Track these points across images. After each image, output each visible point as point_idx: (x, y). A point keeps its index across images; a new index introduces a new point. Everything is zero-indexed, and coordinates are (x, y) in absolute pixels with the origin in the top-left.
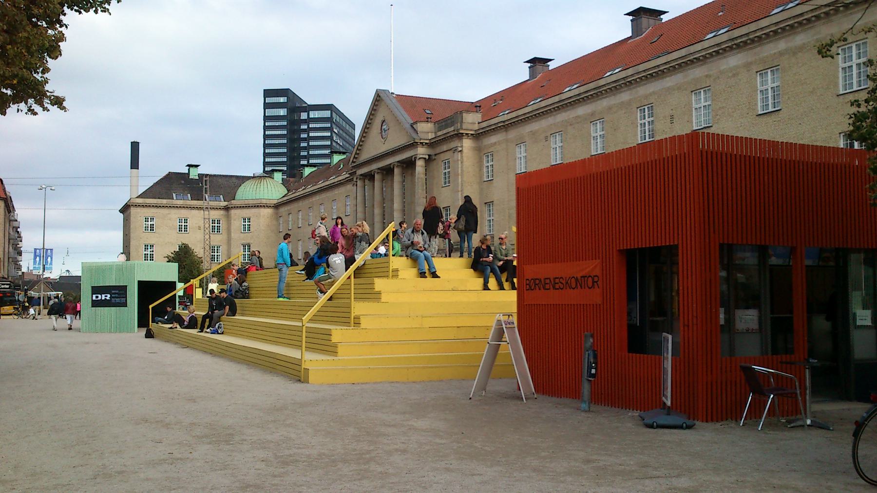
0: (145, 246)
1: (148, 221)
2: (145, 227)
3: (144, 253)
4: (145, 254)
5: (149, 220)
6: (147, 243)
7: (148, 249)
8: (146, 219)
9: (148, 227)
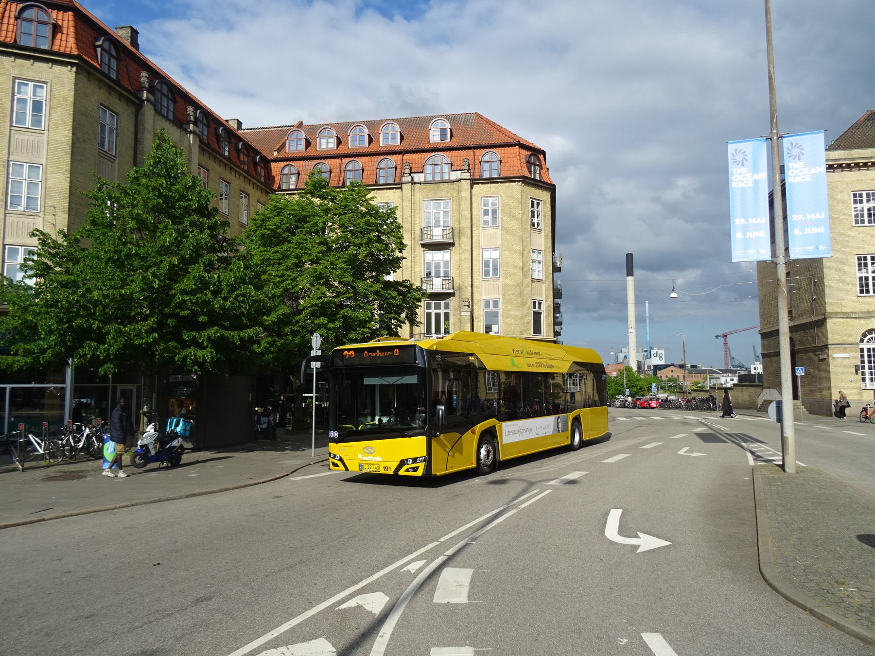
0: (859, 259)
1: (861, 202)
2: (856, 216)
3: (859, 275)
4: (861, 279)
5: (865, 198)
6: (862, 251)
7: (866, 265)
8: (855, 196)
9: (862, 215)
